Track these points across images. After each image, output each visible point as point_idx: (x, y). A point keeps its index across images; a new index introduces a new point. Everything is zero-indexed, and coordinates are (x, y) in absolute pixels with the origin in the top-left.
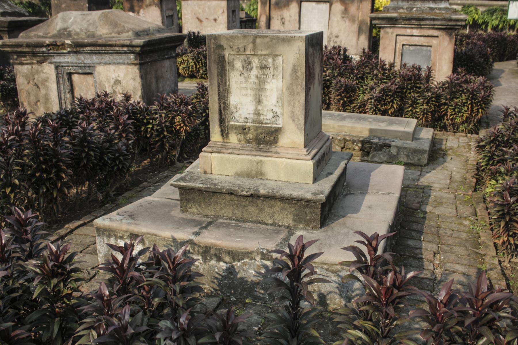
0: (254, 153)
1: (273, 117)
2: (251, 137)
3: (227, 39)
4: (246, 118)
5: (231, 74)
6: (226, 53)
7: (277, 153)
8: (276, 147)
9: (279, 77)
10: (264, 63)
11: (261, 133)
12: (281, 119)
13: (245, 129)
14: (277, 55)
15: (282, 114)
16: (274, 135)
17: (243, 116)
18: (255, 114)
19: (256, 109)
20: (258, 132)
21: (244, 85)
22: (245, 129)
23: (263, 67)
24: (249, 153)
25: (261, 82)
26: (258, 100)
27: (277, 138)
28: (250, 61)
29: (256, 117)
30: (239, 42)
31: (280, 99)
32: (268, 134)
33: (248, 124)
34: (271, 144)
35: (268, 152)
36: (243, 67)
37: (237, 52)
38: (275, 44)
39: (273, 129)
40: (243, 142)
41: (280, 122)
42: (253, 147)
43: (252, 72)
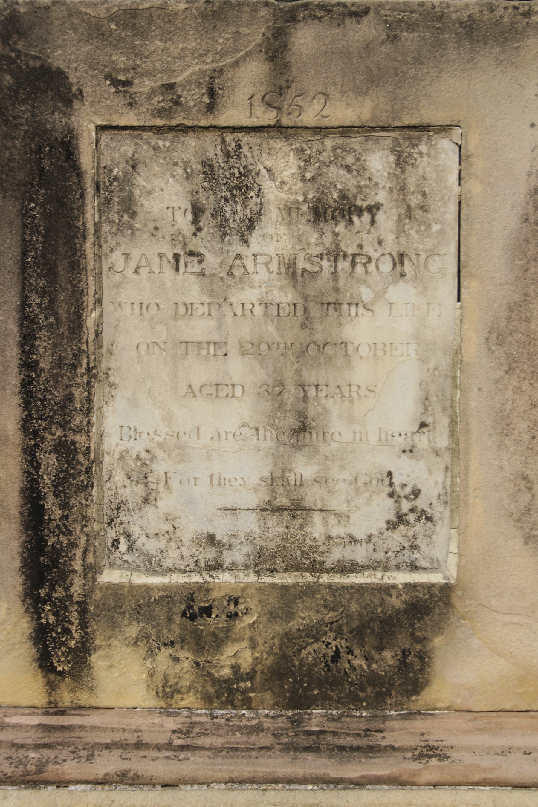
0: (280, 765)
1: (392, 526)
2: (246, 660)
3: (96, 31)
4: (211, 539)
5: (117, 258)
6: (85, 122)
7: (429, 752)
8: (411, 715)
9: (434, 265)
10: (340, 179)
11: (313, 633)
12: (442, 531)
13: (207, 611)
14: (424, 128)
15: (453, 500)
16: (403, 641)
17: (191, 527)
18: (271, 509)
19: (275, 481)
20: (295, 624)
21: (201, 328)
22: (207, 611)
23: (332, 210)
24: (243, 767)
25: (316, 303)
26: (291, 421)
27: (424, 658)
28: (246, 173)
29: (276, 527)
30: (176, 48)
31: (443, 407)
32: (359, 633)
33: (225, 578)
34: (378, 701)
35: (371, 750)
36: (197, 211)
37: (160, 113)
38: (418, 60)
39: (396, 602)
40: (189, 700)
41: (437, 552)
42: (258, 729)
43: (255, 238)
